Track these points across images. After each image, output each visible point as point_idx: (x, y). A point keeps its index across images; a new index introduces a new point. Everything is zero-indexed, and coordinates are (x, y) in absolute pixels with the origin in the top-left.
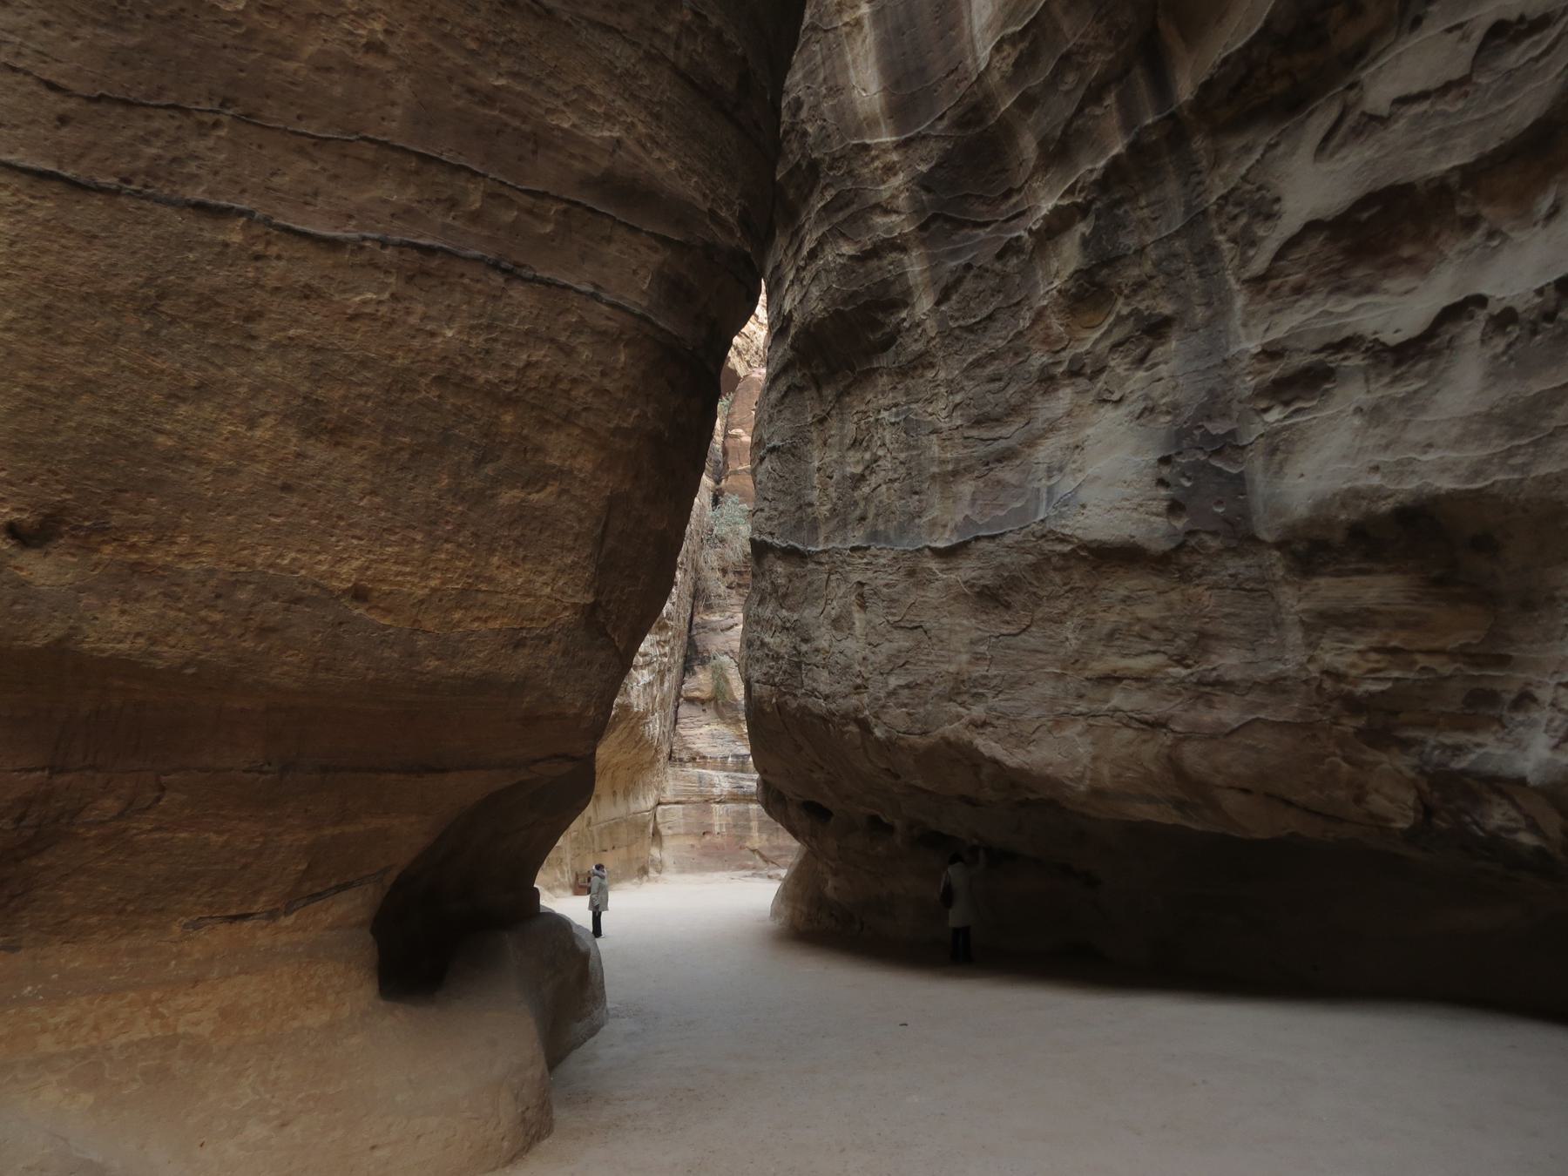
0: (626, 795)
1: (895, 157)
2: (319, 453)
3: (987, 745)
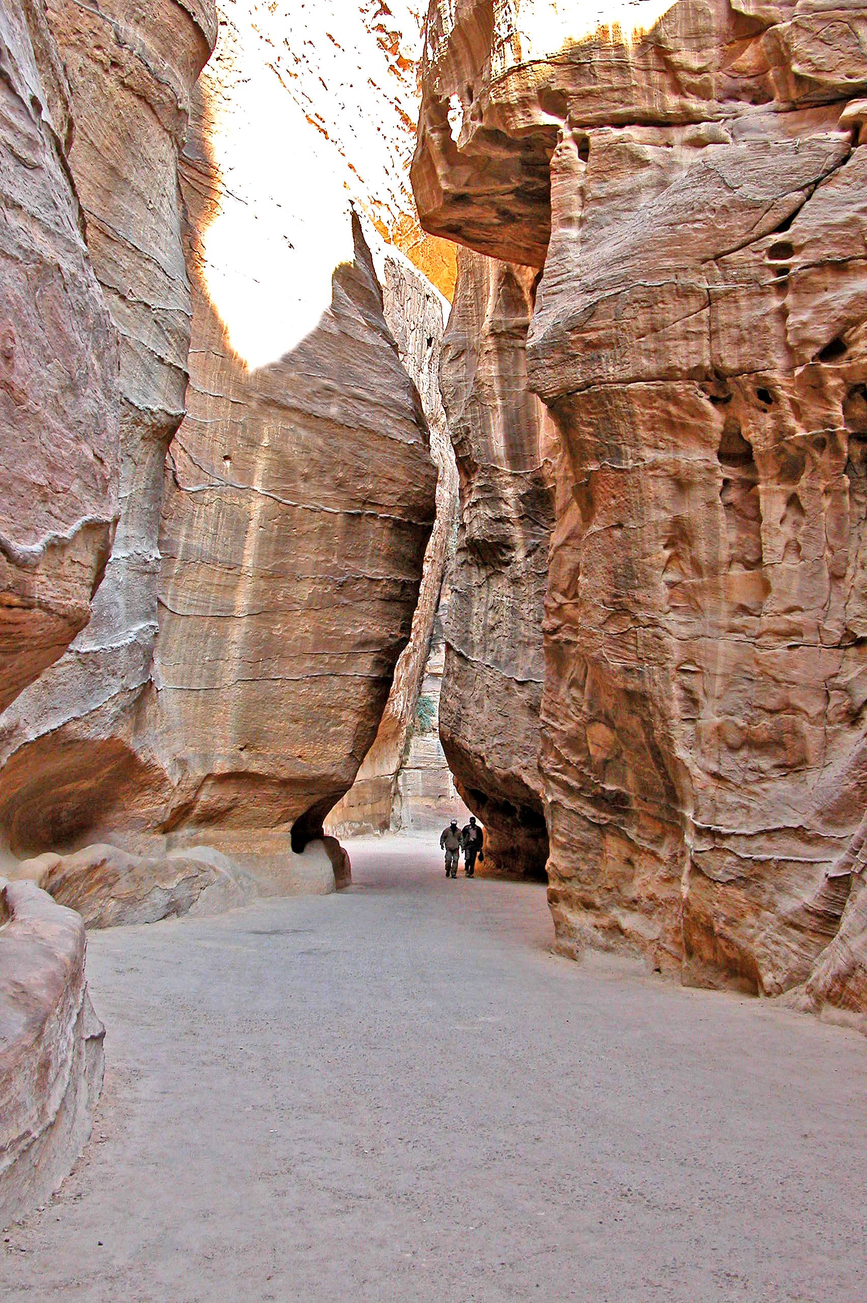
1: (509, 479)
2: (293, 726)
3: (526, 779)
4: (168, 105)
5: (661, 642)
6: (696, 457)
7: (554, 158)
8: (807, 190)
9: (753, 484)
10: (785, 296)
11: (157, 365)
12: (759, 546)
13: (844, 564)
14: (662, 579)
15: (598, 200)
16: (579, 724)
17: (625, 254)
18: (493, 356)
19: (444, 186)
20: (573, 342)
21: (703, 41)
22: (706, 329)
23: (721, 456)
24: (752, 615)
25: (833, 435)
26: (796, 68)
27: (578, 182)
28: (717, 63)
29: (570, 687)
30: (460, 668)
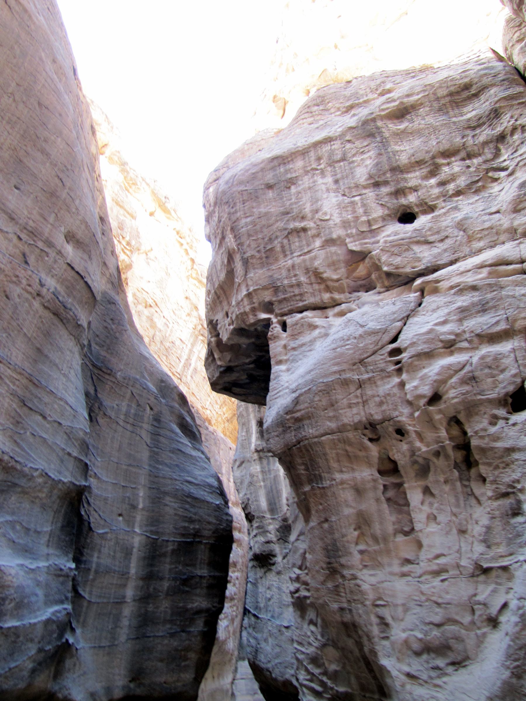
0: (218, 678)
1: (270, 521)
4: (72, 321)
5: (360, 589)
6: (366, 474)
7: (270, 333)
8: (403, 321)
9: (399, 485)
10: (401, 375)
11: (66, 457)
12: (411, 521)
13: (465, 523)
14: (354, 550)
15: (294, 349)
16: (317, 648)
17: (312, 368)
18: (257, 462)
19: (219, 363)
20: (288, 420)
21: (337, 266)
22: (360, 400)
23: (380, 472)
24: (413, 564)
25: (443, 447)
26: (385, 269)
27: (283, 342)
28: (346, 275)
29: (309, 624)
30: (255, 622)
